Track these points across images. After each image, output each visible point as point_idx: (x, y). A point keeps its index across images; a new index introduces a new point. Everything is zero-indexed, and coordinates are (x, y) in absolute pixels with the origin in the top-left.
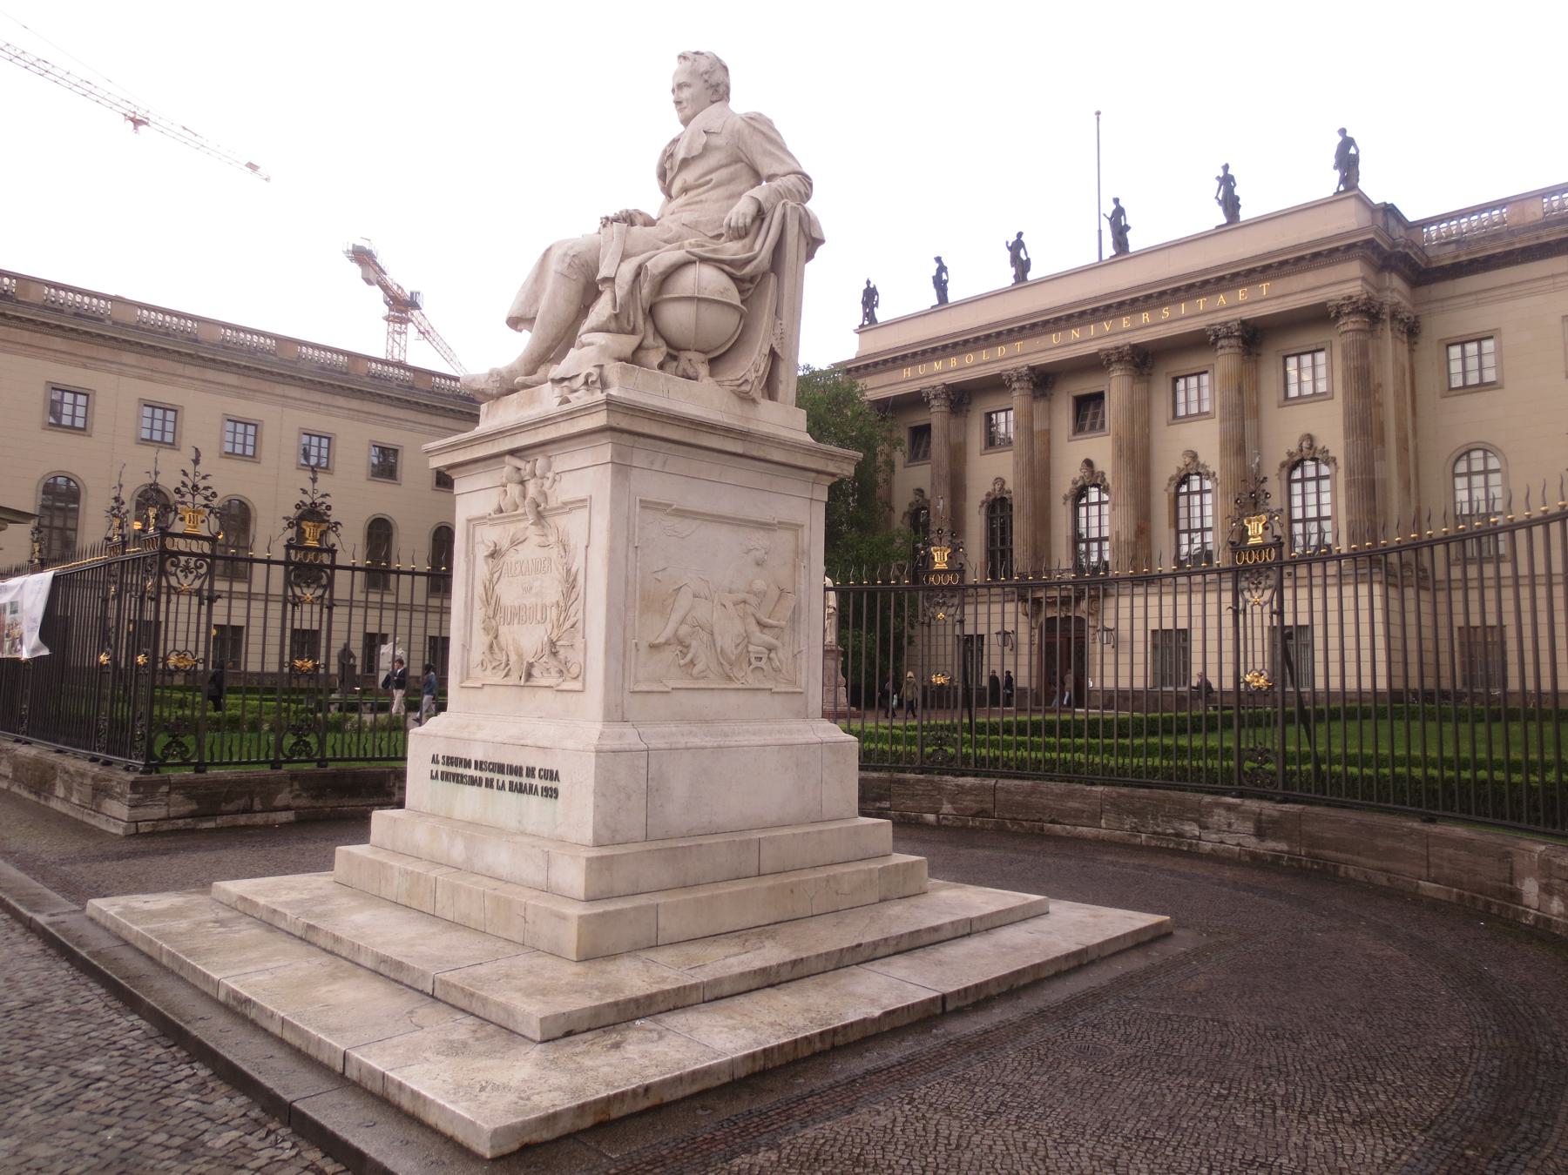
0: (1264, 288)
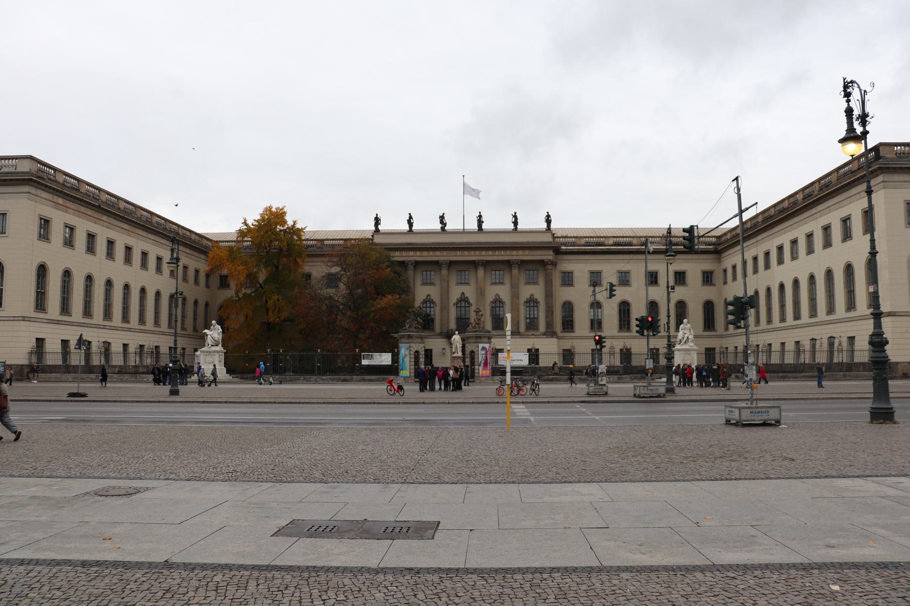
0: (527, 252)
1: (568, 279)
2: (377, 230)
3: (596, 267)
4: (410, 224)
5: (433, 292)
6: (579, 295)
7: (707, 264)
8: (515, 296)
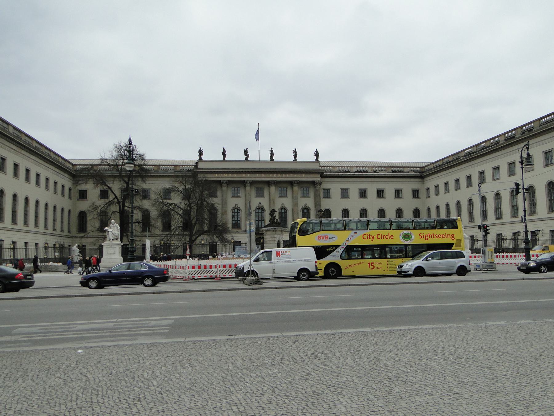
0: (303, 175)
1: (327, 194)
2: (201, 159)
3: (345, 186)
4: (224, 155)
5: (240, 202)
6: (335, 205)
7: (415, 184)
8: (296, 205)
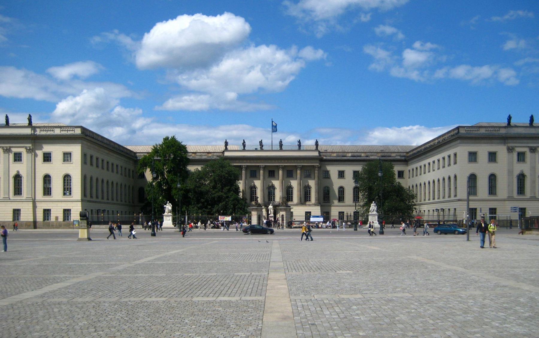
2: (226, 149)
